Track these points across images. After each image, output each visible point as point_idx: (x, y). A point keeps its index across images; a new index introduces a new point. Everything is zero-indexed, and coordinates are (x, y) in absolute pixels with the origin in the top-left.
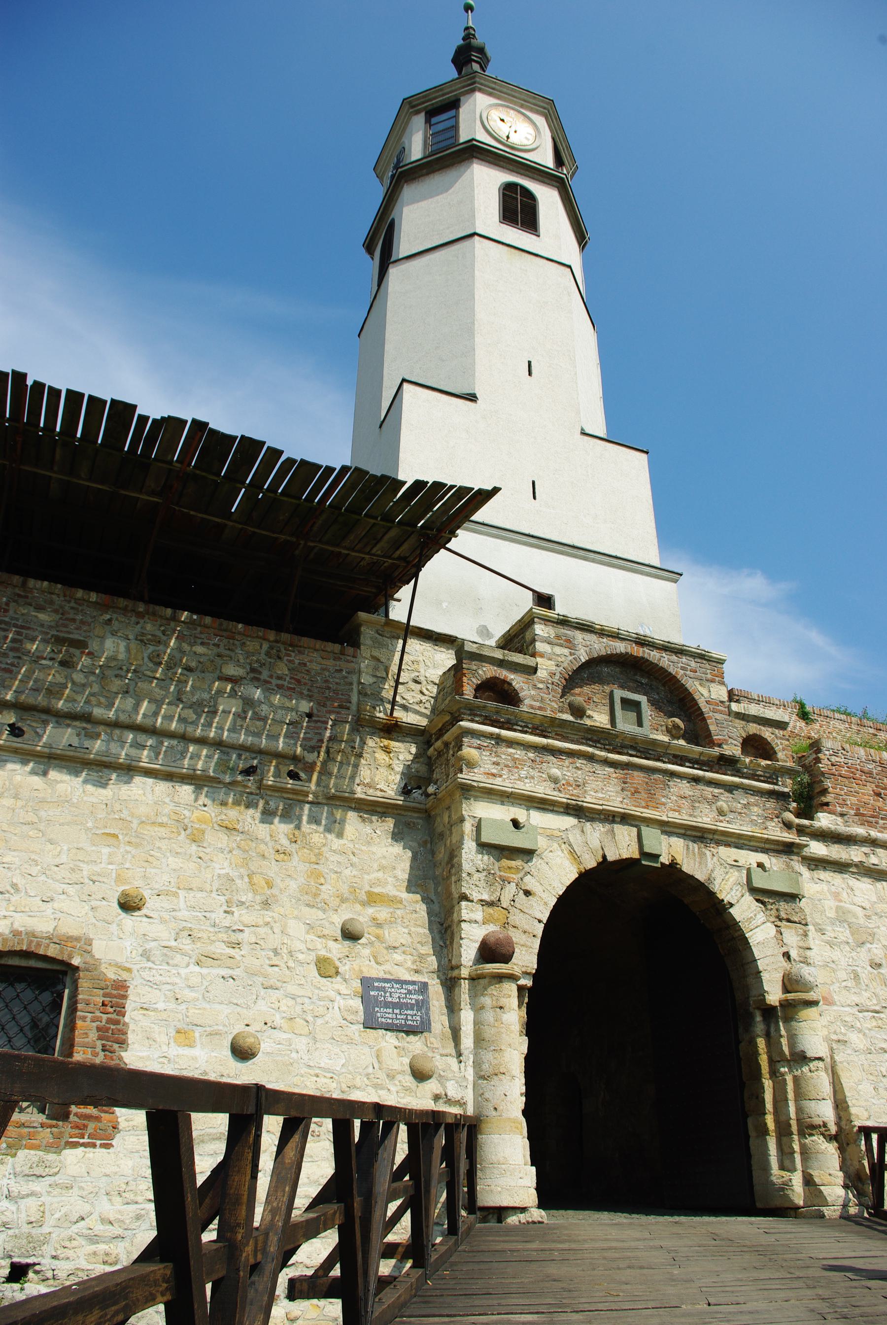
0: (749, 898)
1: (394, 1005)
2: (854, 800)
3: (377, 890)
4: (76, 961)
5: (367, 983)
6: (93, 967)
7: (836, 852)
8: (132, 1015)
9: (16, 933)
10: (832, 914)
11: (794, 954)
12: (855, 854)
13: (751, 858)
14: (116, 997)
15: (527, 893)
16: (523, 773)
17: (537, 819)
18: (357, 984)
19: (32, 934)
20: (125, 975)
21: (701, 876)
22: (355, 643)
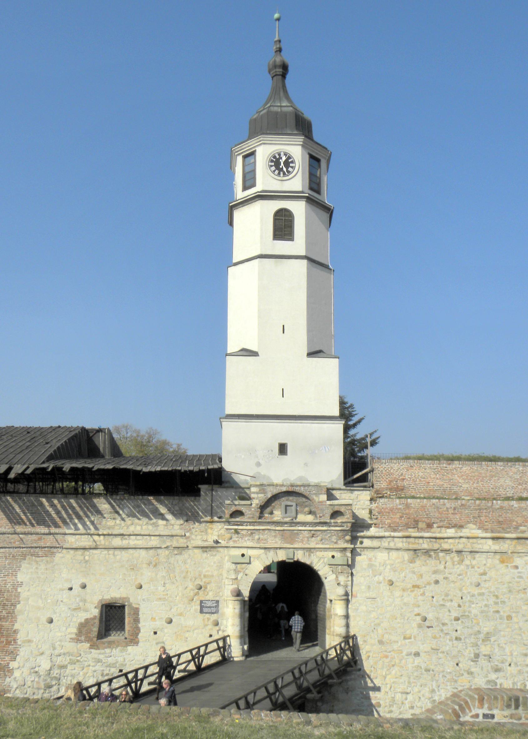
0: (327, 567)
1: (209, 607)
2: (389, 521)
3: (207, 574)
4: (126, 604)
5: (201, 602)
6: (130, 605)
7: (376, 543)
9: (112, 598)
10: (365, 566)
11: (342, 583)
12: (385, 543)
13: (330, 554)
14: (136, 611)
15: (246, 575)
16: (246, 539)
17: (250, 552)
18: (199, 602)
19: (115, 598)
20: (137, 606)
21: (308, 562)
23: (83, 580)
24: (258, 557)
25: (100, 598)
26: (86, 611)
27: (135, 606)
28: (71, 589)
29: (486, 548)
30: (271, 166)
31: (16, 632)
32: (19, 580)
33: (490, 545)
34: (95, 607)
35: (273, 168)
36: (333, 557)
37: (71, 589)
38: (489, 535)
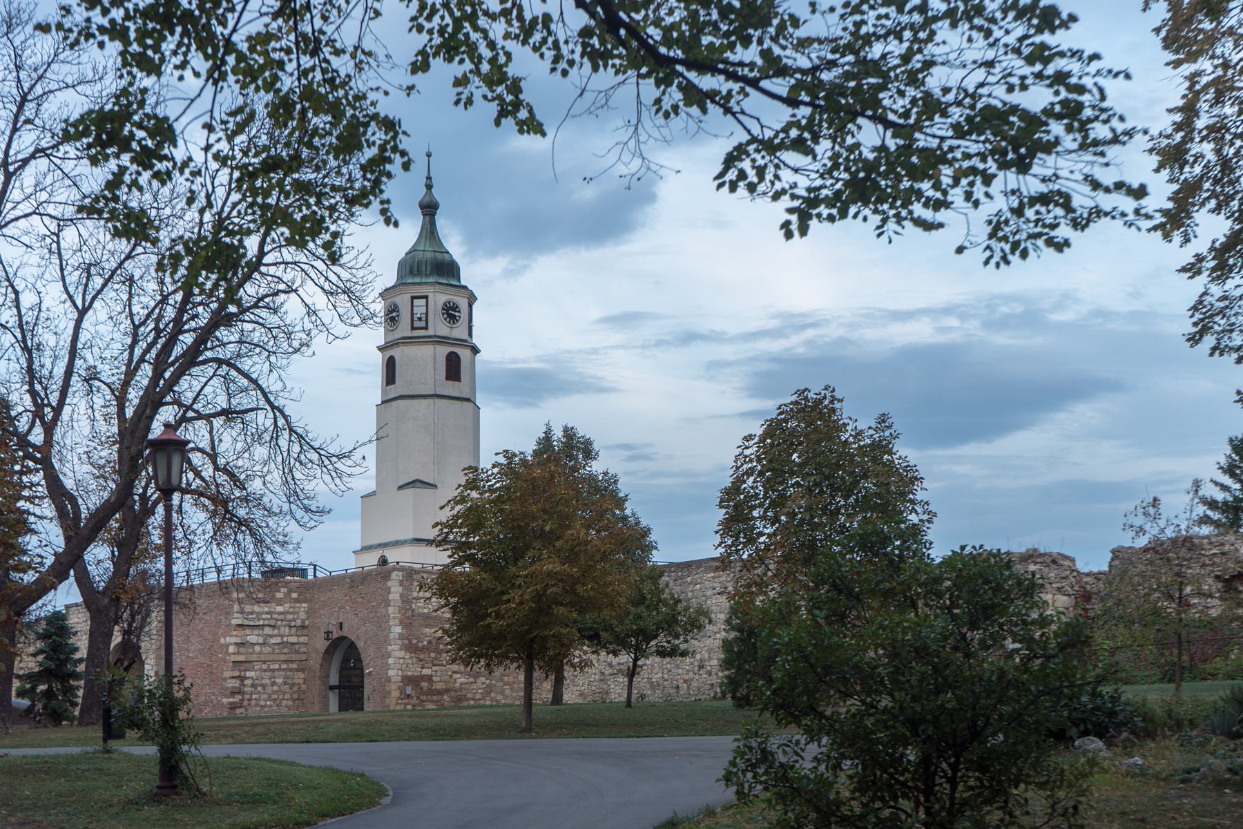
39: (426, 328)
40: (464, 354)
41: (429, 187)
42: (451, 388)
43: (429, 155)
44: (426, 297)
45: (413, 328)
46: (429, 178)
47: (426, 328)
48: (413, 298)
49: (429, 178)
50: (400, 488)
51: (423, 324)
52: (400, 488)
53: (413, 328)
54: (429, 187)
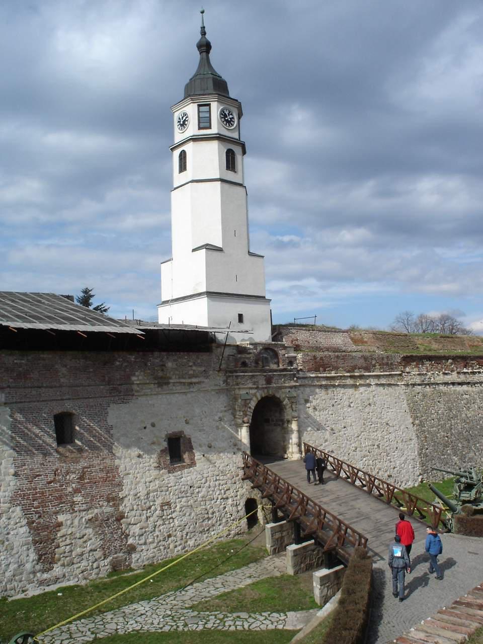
6: (185, 436)
8: (193, 443)
19: (175, 432)
22: (212, 352)
23: (153, 421)
24: (255, 395)
25: (166, 433)
26: (159, 444)
27: (188, 437)
28: (145, 428)
29: (348, 383)
30: (222, 118)
31: (117, 468)
32: (110, 424)
33: (349, 382)
34: (165, 441)
35: (223, 119)
36: (289, 391)
37: (145, 428)
38: (348, 374)
39: (210, 128)
40: (237, 150)
41: (204, 33)
42: (230, 176)
43: (202, 12)
44: (209, 105)
45: (200, 128)
46: (203, 28)
47: (210, 128)
48: (199, 106)
49: (203, 28)
50: (194, 250)
51: (207, 125)
52: (194, 250)
53: (200, 128)
54: (204, 33)
